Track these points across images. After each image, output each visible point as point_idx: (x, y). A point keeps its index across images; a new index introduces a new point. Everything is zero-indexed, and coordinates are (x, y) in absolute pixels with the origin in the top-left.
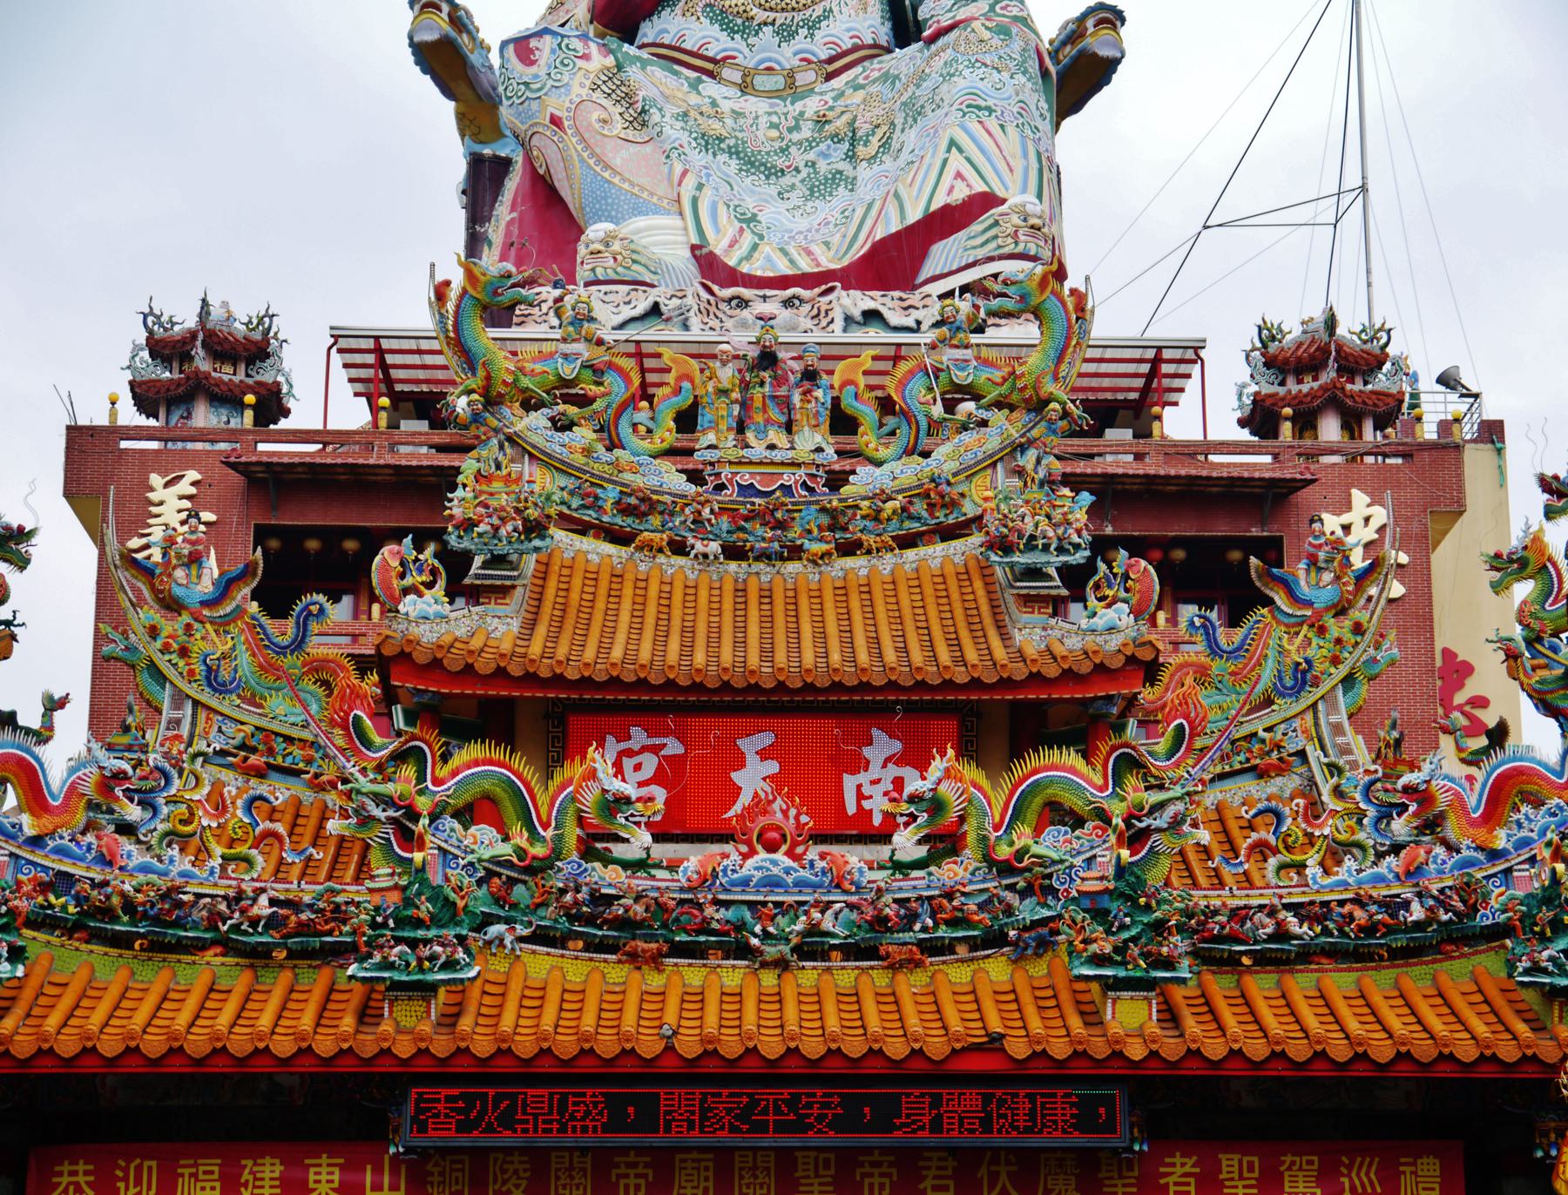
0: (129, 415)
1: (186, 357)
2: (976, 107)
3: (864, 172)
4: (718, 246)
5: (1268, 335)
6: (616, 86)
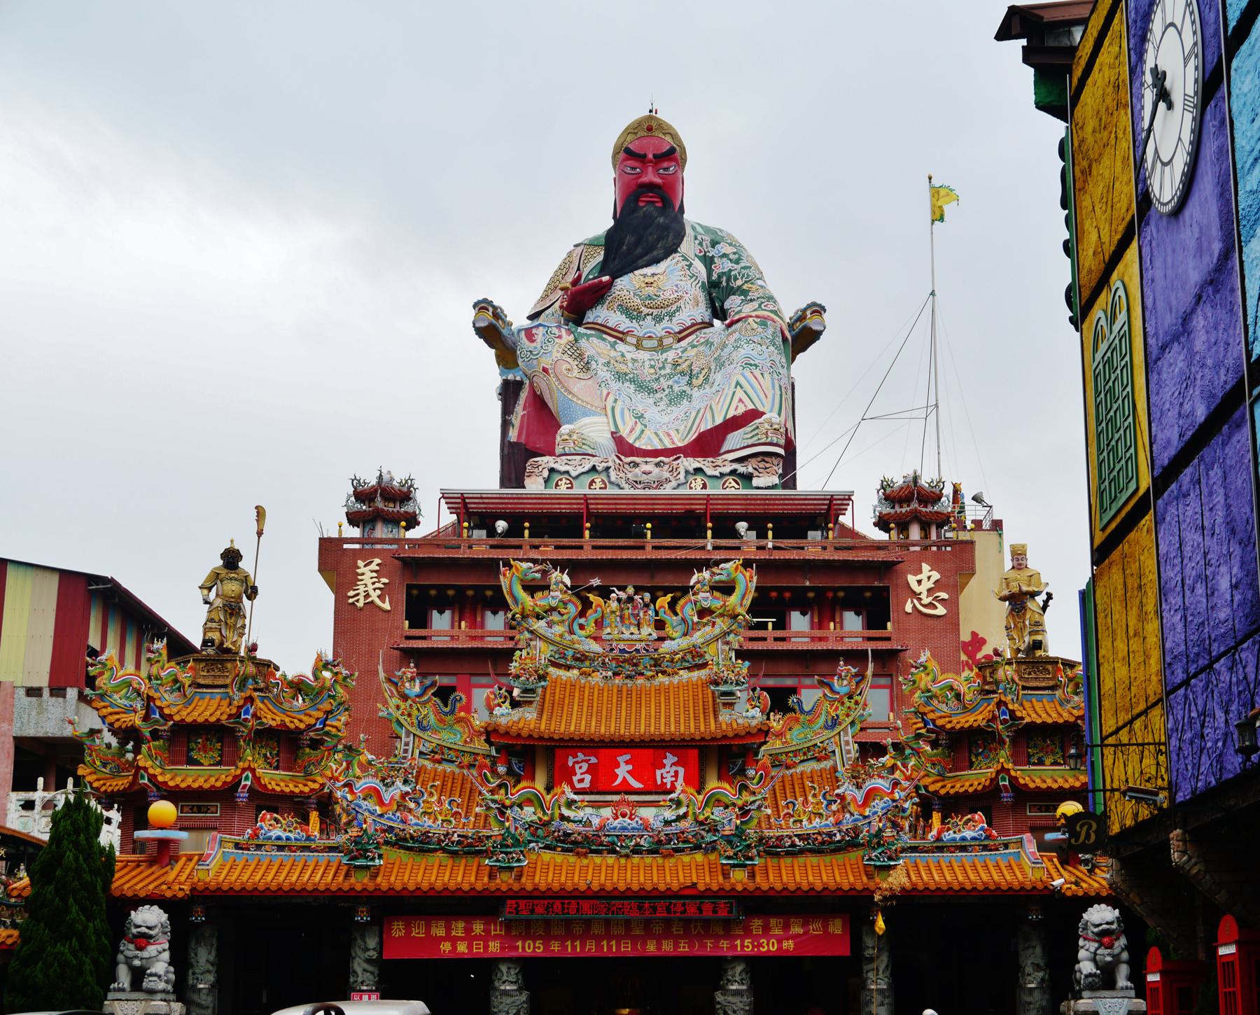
2: (749, 365)
3: (696, 393)
4: (624, 432)
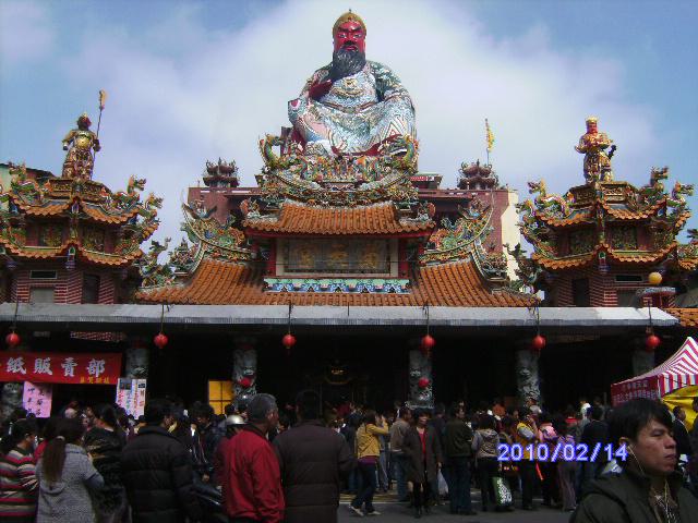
0: (203, 185)
1: (215, 173)
5: (464, 166)
6: (313, 111)
